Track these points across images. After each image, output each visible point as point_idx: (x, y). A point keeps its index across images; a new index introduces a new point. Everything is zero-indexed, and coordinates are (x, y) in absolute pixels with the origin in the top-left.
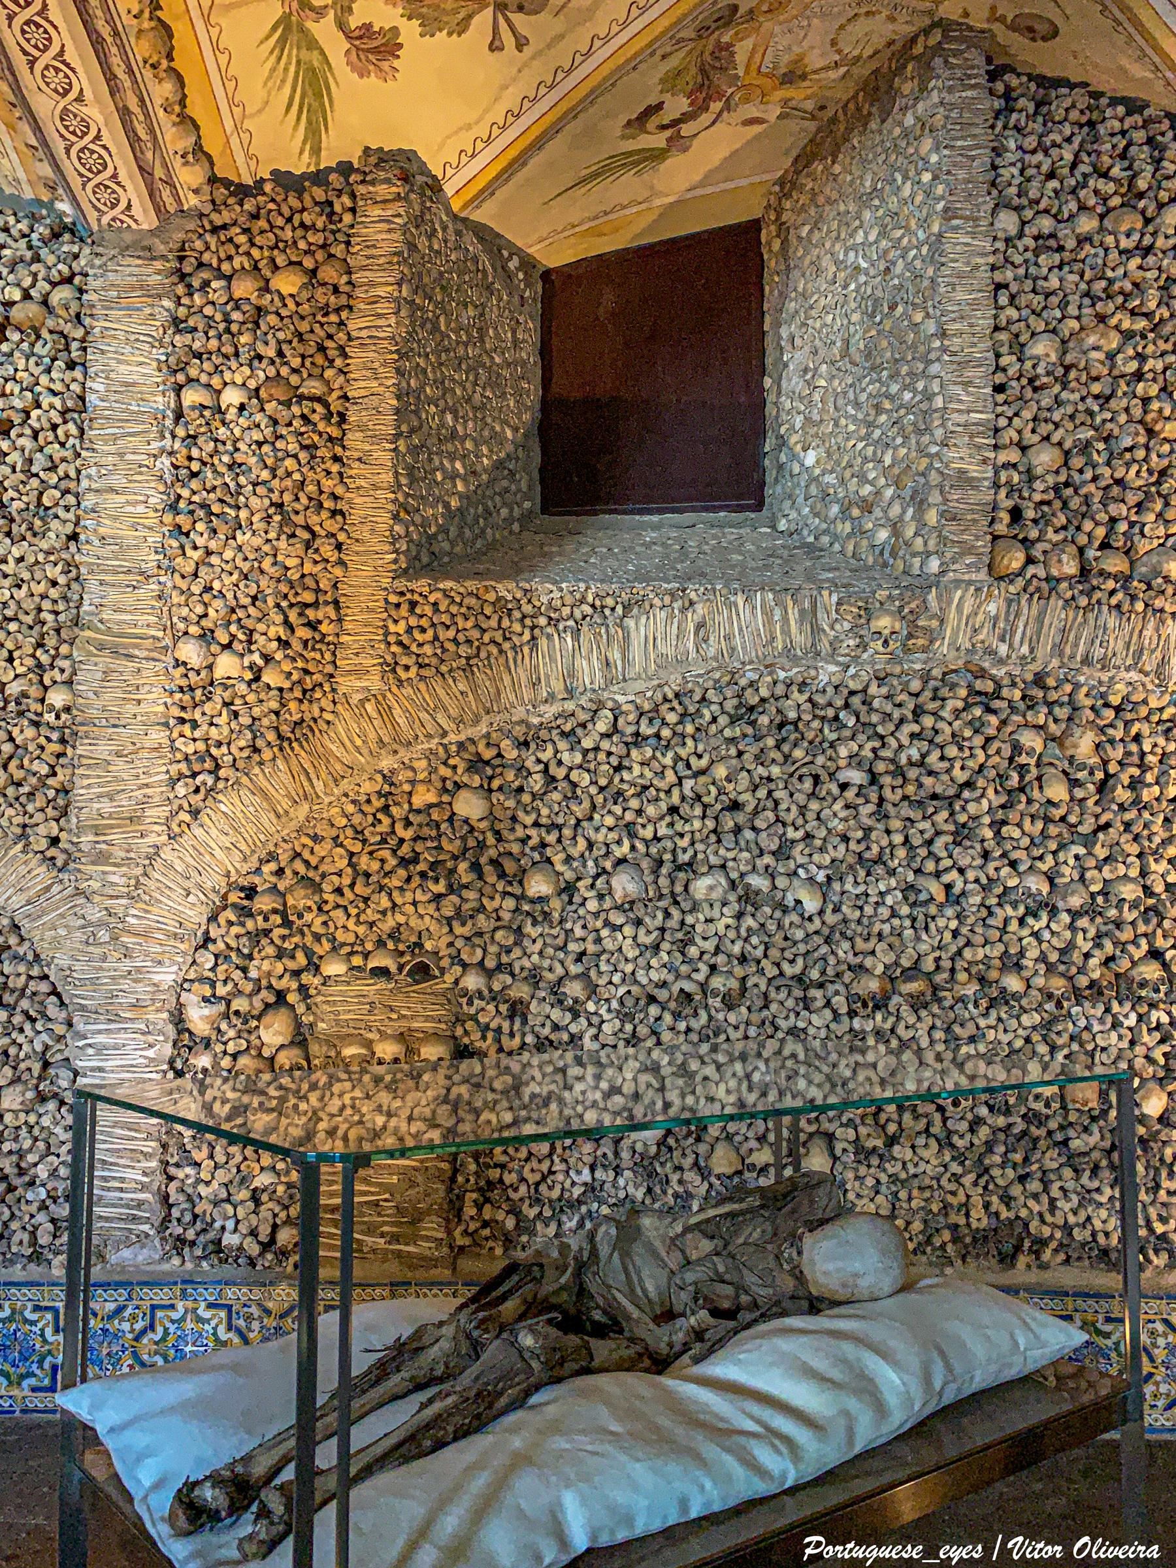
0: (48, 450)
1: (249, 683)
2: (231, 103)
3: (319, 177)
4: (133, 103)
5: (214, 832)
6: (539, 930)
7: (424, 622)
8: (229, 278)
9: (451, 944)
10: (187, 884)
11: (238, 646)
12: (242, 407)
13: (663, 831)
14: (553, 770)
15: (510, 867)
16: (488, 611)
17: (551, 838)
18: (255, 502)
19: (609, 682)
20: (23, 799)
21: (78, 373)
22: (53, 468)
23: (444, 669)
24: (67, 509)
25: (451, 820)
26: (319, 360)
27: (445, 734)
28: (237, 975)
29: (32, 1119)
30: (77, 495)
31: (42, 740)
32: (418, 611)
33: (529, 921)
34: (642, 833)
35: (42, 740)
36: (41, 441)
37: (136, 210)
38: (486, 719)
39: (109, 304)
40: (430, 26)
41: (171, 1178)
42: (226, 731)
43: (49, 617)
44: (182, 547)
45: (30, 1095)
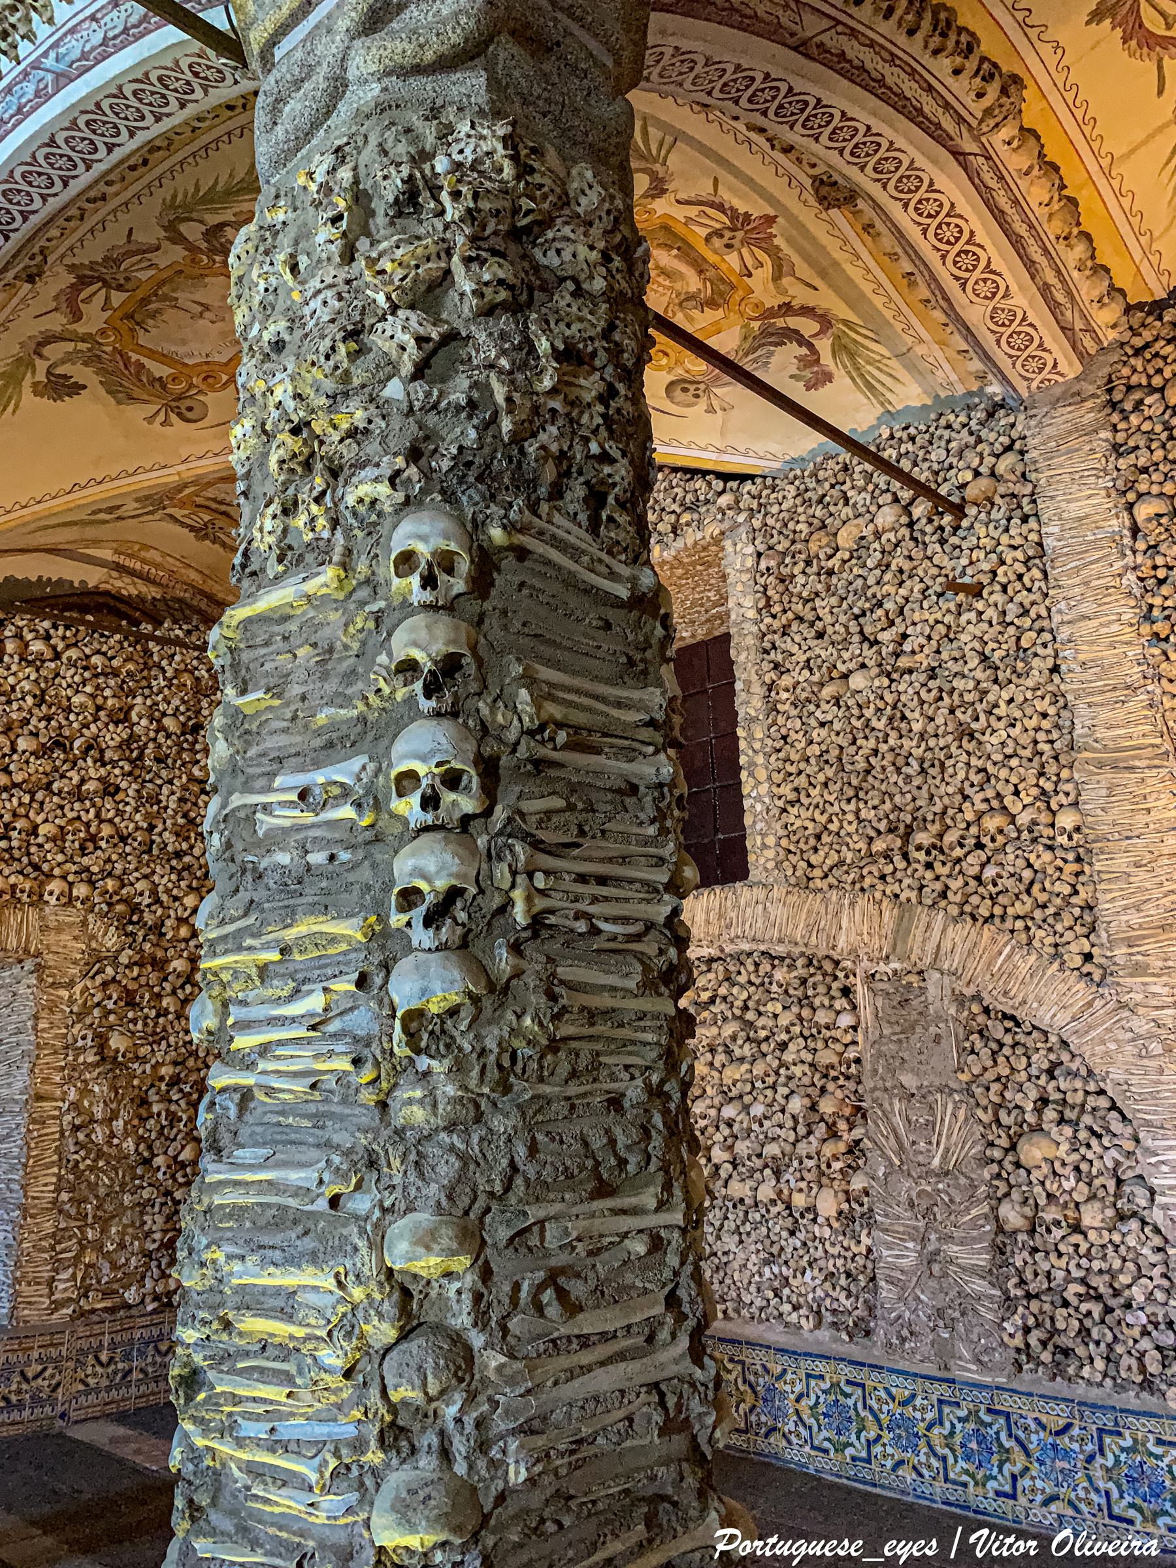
0: (1018, 599)
20: (1050, 920)
21: (1033, 524)
22: (1026, 613)
24: (1045, 646)
29: (1117, 1238)
30: (1051, 631)
31: (1059, 863)
35: (1059, 863)
36: (1010, 591)
39: (1050, 455)
43: (1045, 747)
44: (1165, 653)
45: (1110, 1212)
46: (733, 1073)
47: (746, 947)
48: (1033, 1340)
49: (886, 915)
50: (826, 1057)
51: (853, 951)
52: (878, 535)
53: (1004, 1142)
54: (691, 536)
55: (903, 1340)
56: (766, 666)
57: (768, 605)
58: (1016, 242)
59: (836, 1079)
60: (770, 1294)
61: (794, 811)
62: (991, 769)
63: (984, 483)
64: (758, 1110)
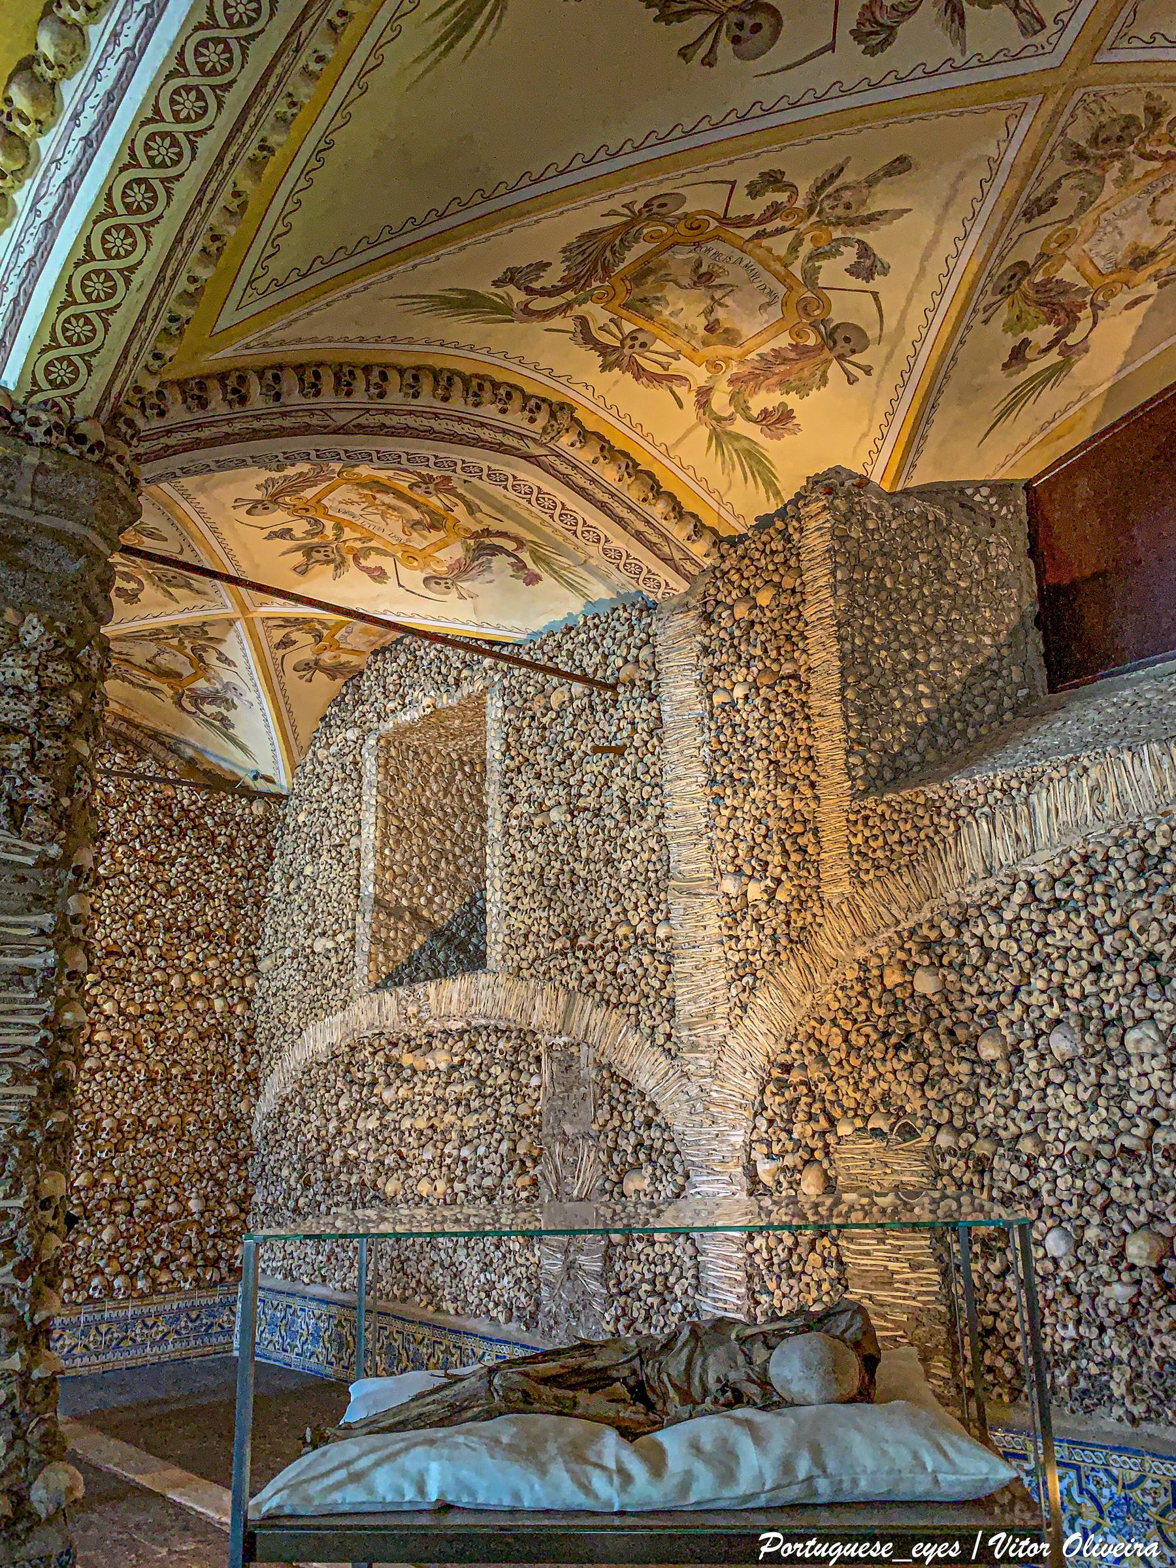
1: (768, 902)
2: (709, 493)
3: (781, 514)
4: (641, 526)
5: (757, 1022)
6: (993, 1090)
7: (875, 831)
8: (731, 607)
9: (925, 1107)
10: (743, 1064)
11: (757, 875)
12: (746, 697)
13: (1089, 989)
14: (987, 942)
15: (961, 1034)
16: (920, 812)
17: (992, 1005)
18: (758, 765)
19: (1020, 857)
21: (655, 704)
23: (893, 867)
24: (656, 797)
25: (912, 996)
26: (788, 647)
27: (898, 922)
28: (783, 1136)
32: (871, 823)
33: (982, 1085)
34: (1069, 991)
37: (672, 584)
38: (926, 905)
39: (669, 650)
40: (802, 390)
41: (758, 1303)
42: (756, 941)
46: (471, 1121)
47: (483, 1022)
48: (620, 1326)
49: (560, 999)
50: (524, 1110)
51: (540, 1027)
52: (571, 700)
53: (614, 1178)
54: (466, 688)
55: (551, 1328)
56: (504, 798)
57: (508, 749)
58: (602, 507)
59: (528, 1127)
60: (483, 1295)
61: (513, 914)
62: (621, 890)
63: (629, 668)
64: (481, 1151)
